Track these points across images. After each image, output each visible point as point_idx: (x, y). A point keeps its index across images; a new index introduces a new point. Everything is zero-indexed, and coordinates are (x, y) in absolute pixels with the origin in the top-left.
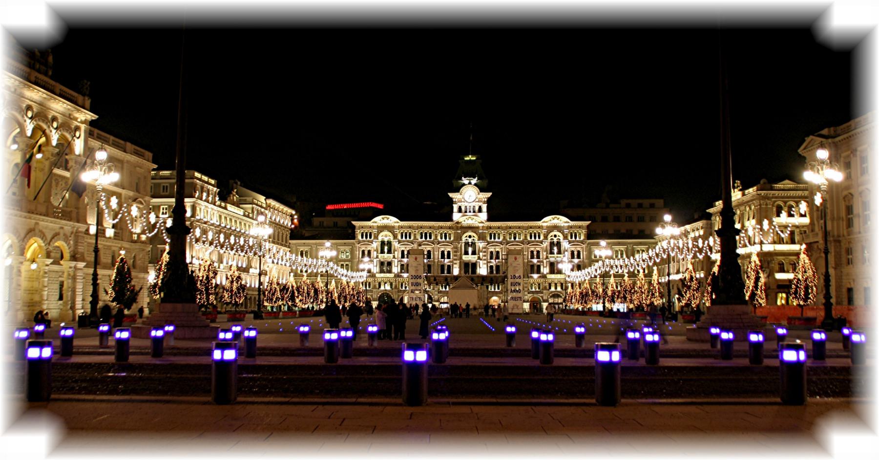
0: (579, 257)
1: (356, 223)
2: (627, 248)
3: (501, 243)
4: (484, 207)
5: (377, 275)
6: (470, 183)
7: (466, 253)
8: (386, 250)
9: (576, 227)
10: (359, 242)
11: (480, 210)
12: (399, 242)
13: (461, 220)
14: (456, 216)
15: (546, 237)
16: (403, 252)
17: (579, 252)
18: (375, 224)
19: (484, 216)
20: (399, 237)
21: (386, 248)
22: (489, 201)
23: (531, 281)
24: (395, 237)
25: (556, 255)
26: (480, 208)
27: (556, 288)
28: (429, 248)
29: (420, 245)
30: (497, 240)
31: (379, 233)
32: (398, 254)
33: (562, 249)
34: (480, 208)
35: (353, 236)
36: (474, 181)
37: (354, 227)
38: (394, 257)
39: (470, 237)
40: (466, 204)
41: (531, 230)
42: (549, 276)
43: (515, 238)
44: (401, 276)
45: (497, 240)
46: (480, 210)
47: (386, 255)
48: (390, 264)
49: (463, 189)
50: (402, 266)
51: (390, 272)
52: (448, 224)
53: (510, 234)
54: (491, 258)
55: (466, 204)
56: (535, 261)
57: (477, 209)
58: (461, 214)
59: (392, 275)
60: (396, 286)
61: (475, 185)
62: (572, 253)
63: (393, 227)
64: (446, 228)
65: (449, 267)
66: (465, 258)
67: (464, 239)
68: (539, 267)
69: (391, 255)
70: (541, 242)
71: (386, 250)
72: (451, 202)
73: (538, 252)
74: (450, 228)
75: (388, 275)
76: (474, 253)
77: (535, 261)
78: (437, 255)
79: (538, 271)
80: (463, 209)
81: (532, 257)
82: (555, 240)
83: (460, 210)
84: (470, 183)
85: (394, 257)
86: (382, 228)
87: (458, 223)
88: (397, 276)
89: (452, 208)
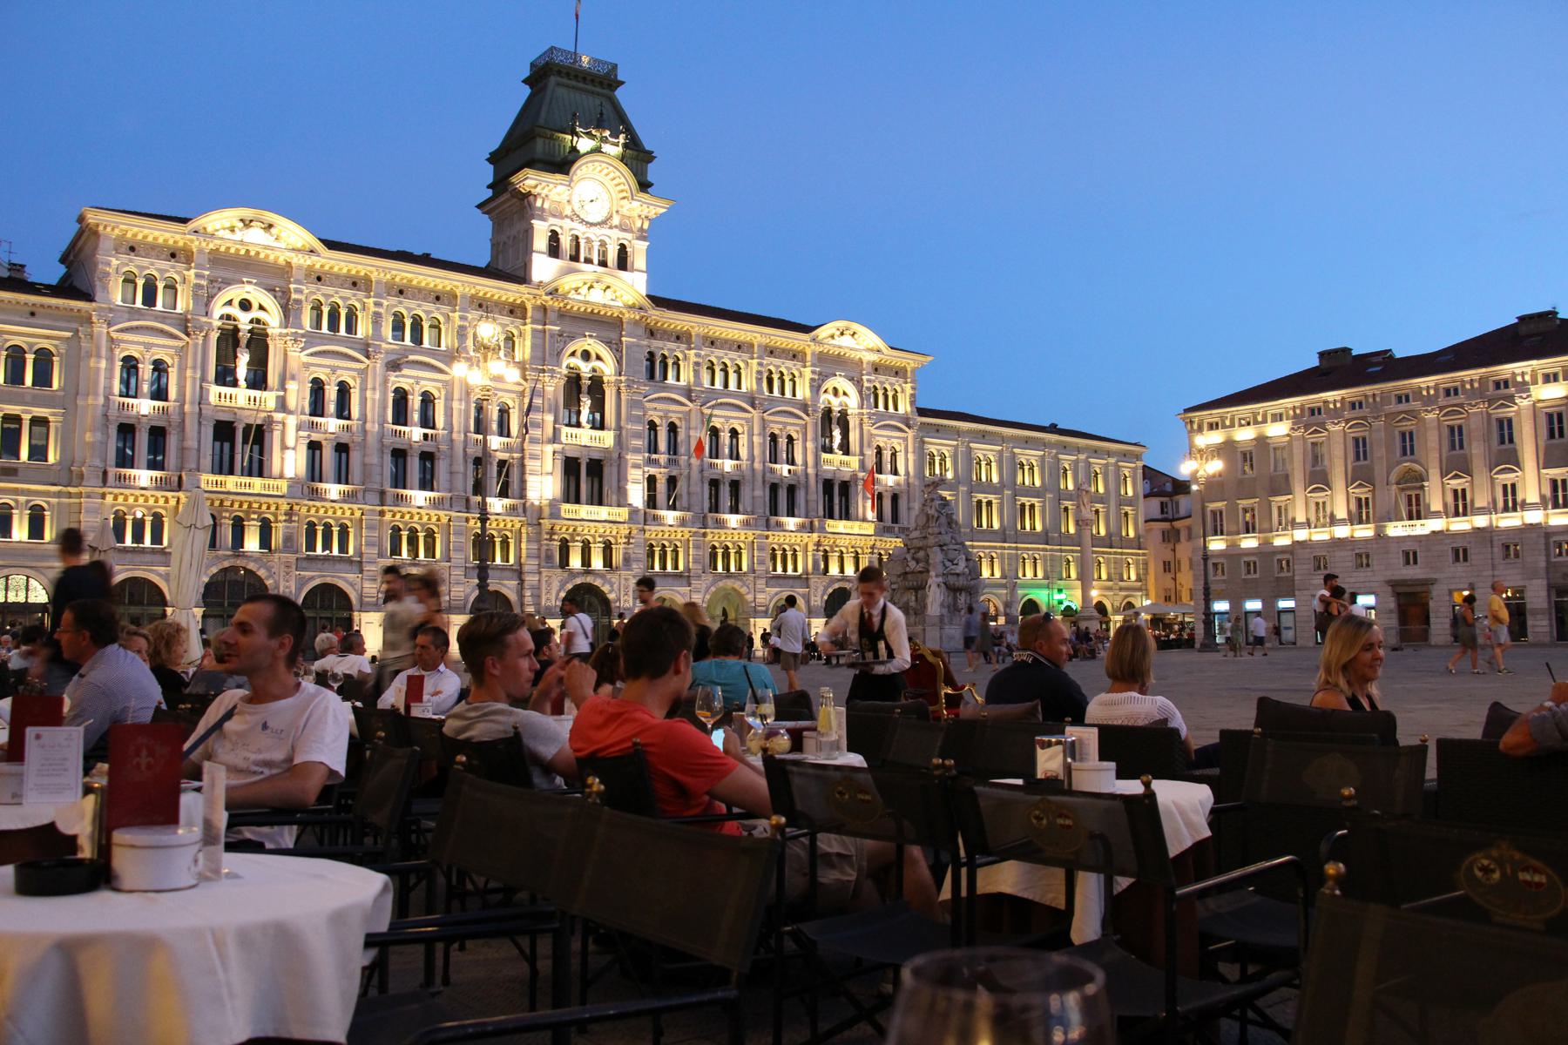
8: (242, 371)
11: (623, 263)
13: (567, 283)
14: (543, 268)
16: (318, 388)
18: (196, 244)
23: (776, 538)
29: (394, 366)
31: (216, 284)
32: (298, 395)
33: (854, 436)
38: (282, 405)
44: (315, 494)
46: (623, 263)
48: (259, 435)
49: (581, 170)
51: (258, 468)
55: (581, 230)
59: (284, 486)
60: (288, 539)
71: (242, 371)
80: (566, 243)
83: (554, 250)
85: (282, 405)
89: (528, 233)
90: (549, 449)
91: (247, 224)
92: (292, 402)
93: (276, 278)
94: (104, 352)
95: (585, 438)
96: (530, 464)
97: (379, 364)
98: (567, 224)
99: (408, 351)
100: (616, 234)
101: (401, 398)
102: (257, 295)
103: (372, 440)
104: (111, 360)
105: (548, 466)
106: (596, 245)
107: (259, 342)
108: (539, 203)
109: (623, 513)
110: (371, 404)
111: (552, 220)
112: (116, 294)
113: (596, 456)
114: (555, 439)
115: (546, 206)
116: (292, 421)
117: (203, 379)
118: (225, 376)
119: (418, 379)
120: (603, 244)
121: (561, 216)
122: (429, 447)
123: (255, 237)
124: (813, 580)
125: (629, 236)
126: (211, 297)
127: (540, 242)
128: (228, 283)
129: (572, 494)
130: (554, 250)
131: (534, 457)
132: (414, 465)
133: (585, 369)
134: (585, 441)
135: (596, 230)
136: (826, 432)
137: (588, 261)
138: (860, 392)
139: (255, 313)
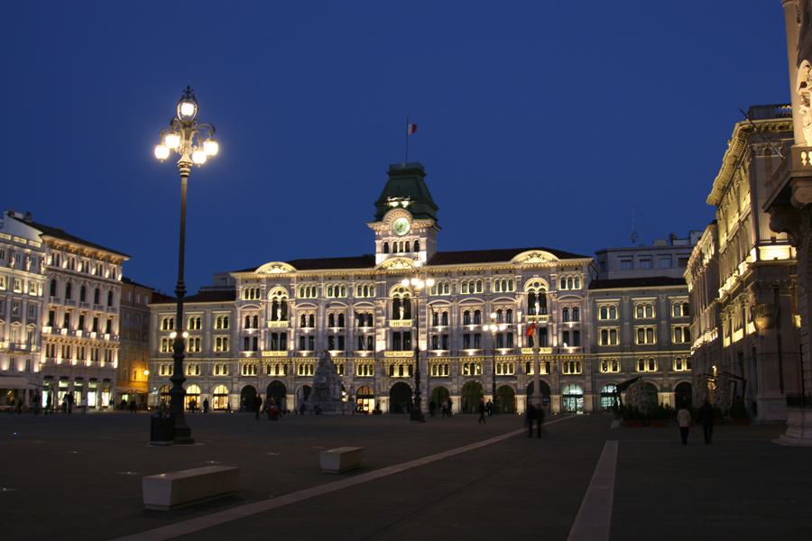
0: (575, 318)
1: (239, 276)
2: (621, 302)
3: (449, 298)
4: (423, 240)
5: (264, 354)
6: (400, 206)
7: (396, 317)
9: (570, 268)
10: (241, 303)
11: (417, 248)
12: (297, 301)
14: (381, 259)
15: (521, 287)
17: (576, 310)
18: (261, 276)
19: (423, 256)
20: (298, 295)
21: (279, 311)
22: (430, 233)
24: (291, 293)
25: (537, 316)
26: (417, 244)
27: (277, 372)
28: (340, 310)
29: (328, 306)
30: (443, 294)
32: (296, 321)
33: (548, 304)
34: (417, 244)
35: (231, 295)
36: (405, 204)
37: (234, 280)
39: (537, 285)
40: (396, 239)
41: (497, 277)
42: (387, 354)
43: (472, 291)
44: (300, 355)
45: (443, 294)
46: (417, 248)
47: (279, 324)
48: (284, 336)
49: (389, 215)
50: (302, 338)
51: (284, 348)
52: (367, 271)
53: (464, 285)
54: (566, 319)
56: (251, 331)
57: (412, 245)
58: (386, 255)
61: (409, 208)
62: (565, 310)
63: (289, 280)
64: (366, 277)
65: (370, 338)
66: (392, 323)
67: (392, 295)
68: (256, 340)
69: (286, 323)
70: (514, 295)
71: (279, 316)
72: (372, 236)
73: (256, 318)
74: (372, 277)
75: (279, 353)
76: (407, 316)
77: (251, 331)
78: (352, 321)
79: (371, 347)
80: (391, 246)
81: (247, 326)
82: (279, 299)
83: (386, 250)
84: (400, 206)
85: (290, 326)
86: (273, 281)
87: (381, 268)
88: (296, 354)
90: (383, 330)
91: (273, 267)
92: (555, 318)
93: (285, 281)
94: (239, 315)
95: (402, 323)
96: (377, 337)
97: (322, 307)
98: (390, 238)
99: (333, 300)
100: (412, 237)
101: (331, 316)
102: (283, 290)
103: (320, 333)
104: (241, 317)
105: (383, 336)
106: (404, 244)
107: (284, 305)
108: (377, 233)
109: (285, 353)
110: (322, 321)
111: (384, 239)
112: (242, 297)
113: (406, 330)
114: (387, 324)
115: (380, 233)
116: (293, 331)
117: (266, 320)
118: (274, 318)
119: (336, 310)
120: (407, 243)
121: (387, 235)
122: (341, 334)
123: (277, 271)
124: (519, 376)
125: (418, 237)
126: (267, 293)
127: (379, 249)
128: (273, 287)
129: (396, 347)
130: (386, 250)
131: (379, 334)
132: (336, 341)
133: (402, 296)
134: (401, 325)
135: (404, 238)
136: (531, 305)
137: (401, 251)
138: (550, 283)
139: (283, 296)
